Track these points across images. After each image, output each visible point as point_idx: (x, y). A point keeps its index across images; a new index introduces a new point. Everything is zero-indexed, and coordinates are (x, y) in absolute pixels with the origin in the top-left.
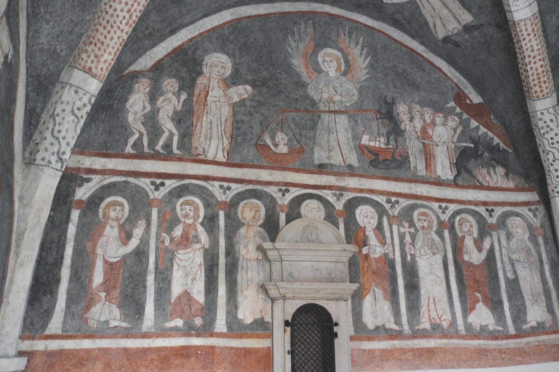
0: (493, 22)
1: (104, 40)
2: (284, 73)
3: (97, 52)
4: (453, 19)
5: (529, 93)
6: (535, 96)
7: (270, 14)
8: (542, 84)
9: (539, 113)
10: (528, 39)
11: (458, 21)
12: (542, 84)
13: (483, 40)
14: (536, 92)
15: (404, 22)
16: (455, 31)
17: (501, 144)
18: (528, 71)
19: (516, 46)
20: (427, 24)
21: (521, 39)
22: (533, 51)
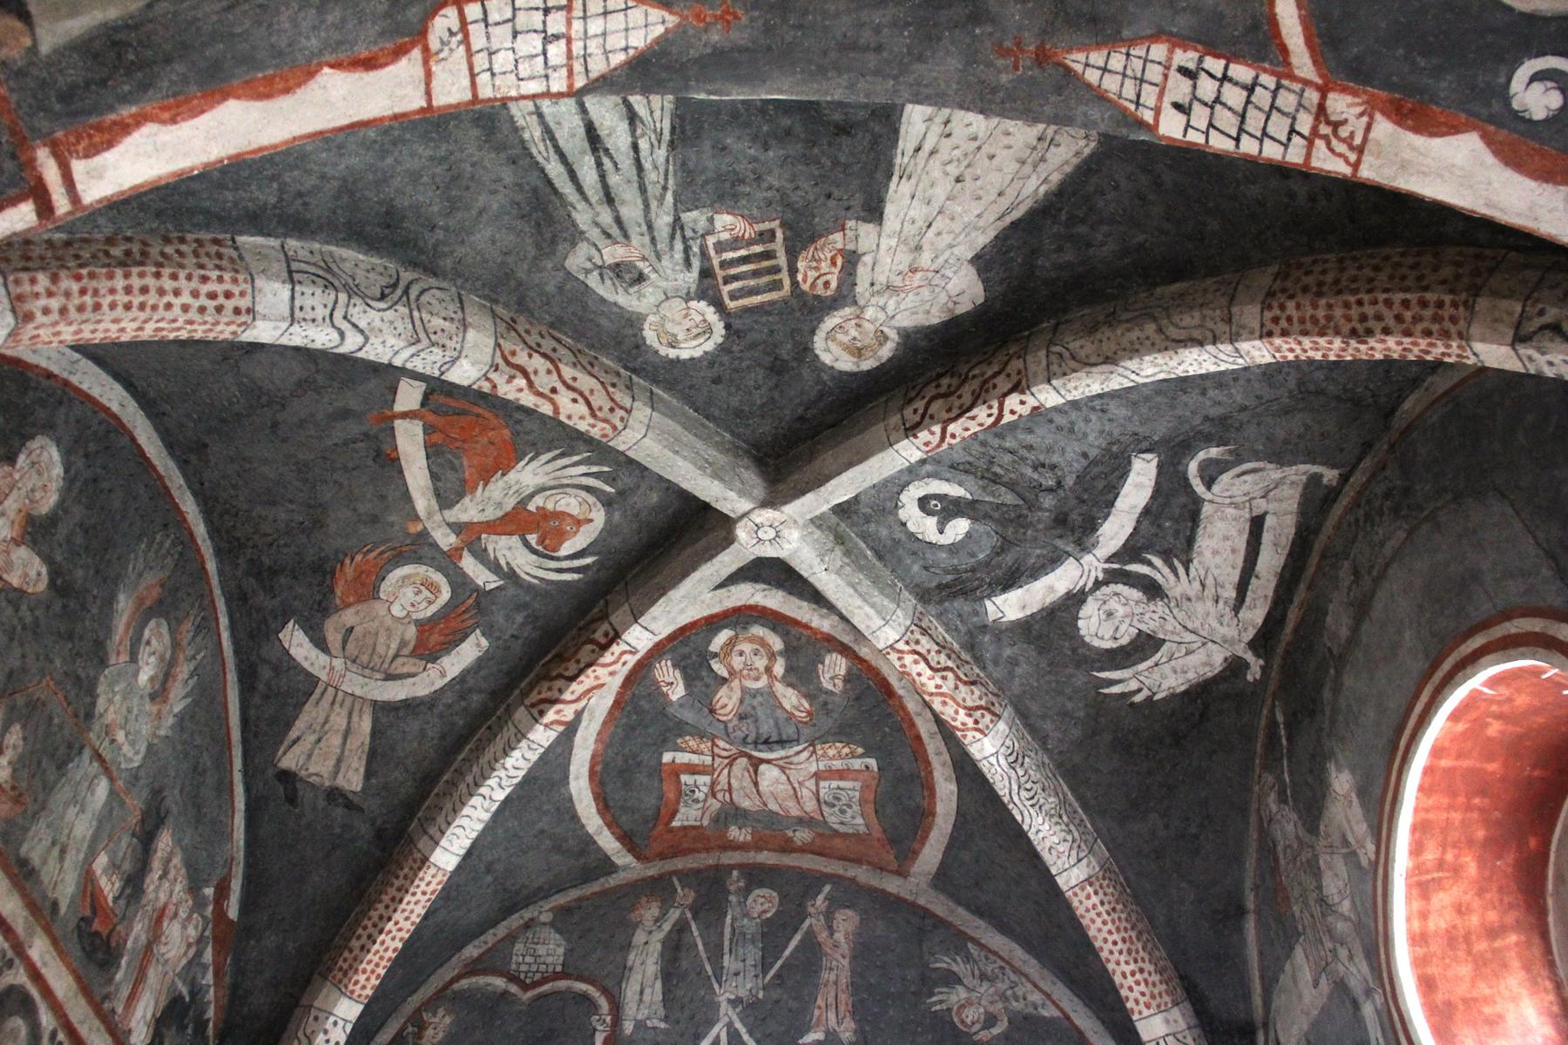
0: (379, 821)
1: (105, 307)
2: (98, 602)
3: (72, 309)
4: (332, 763)
5: (345, 974)
6: (351, 987)
7: (154, 468)
8: (373, 977)
9: (332, 1019)
10: (419, 896)
11: (336, 773)
12: (373, 977)
13: (338, 831)
14: (356, 983)
15: (261, 686)
16: (312, 779)
17: (211, 1025)
18: (374, 942)
19: (392, 892)
20: (289, 725)
21: (412, 890)
22: (407, 919)
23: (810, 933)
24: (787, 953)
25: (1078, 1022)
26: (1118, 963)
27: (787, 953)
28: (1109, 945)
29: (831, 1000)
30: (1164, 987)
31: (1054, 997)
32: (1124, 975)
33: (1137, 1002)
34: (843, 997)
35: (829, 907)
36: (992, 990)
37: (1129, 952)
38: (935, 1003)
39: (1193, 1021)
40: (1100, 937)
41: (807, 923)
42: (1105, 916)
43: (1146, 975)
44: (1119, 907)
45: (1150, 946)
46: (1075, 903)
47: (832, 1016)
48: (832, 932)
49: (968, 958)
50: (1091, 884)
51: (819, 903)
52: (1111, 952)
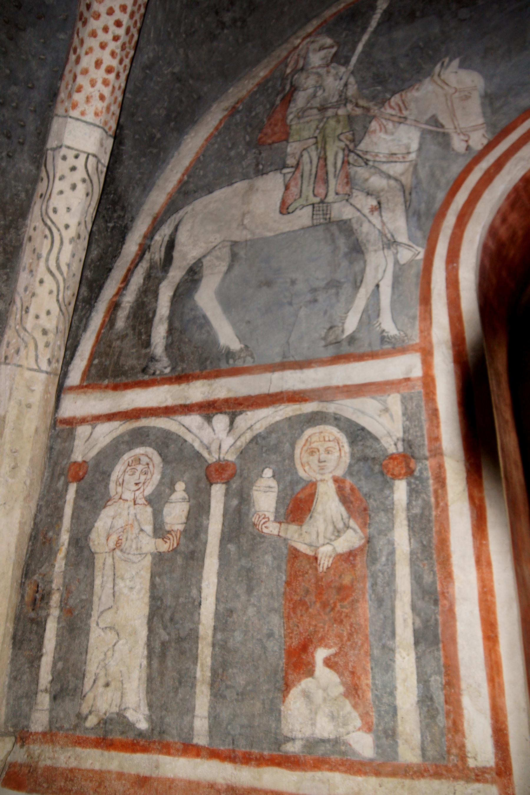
26: (103, 46)
28: (110, 21)
32: (98, 64)
33: (88, 100)
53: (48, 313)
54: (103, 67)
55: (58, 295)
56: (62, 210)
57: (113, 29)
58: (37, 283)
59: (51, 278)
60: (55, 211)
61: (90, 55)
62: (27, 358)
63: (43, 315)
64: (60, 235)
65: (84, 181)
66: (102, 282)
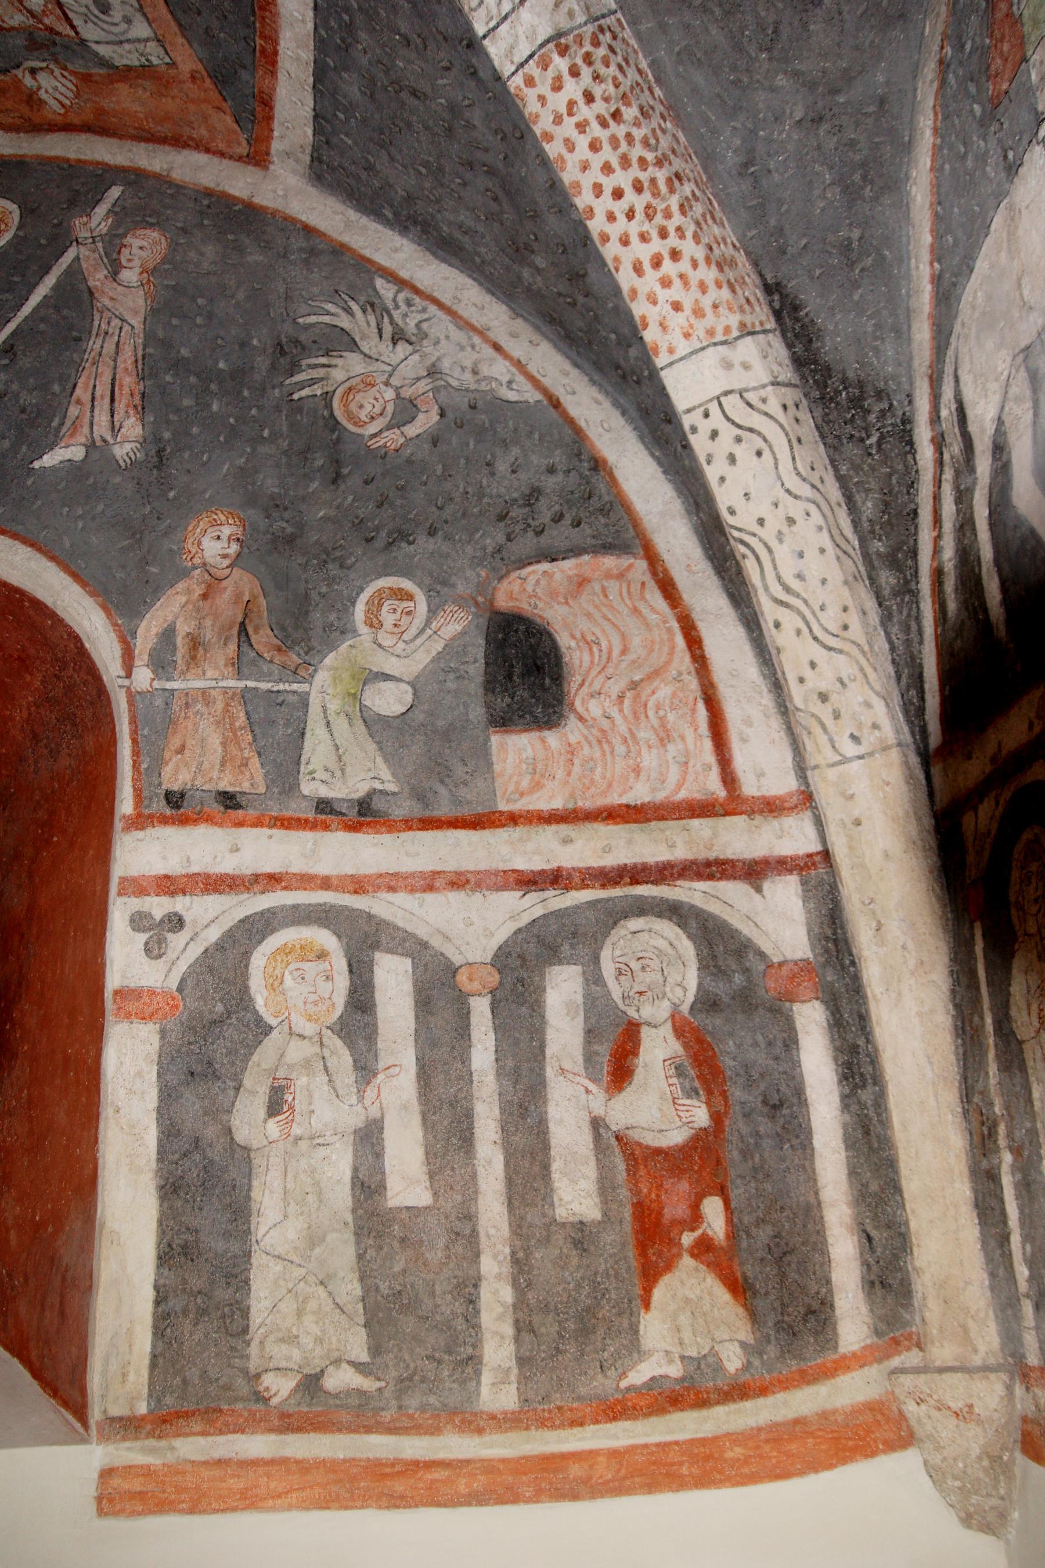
23: (74, 272)
24: (27, 309)
25: (574, 411)
26: (625, 242)
27: (27, 309)
29: (103, 389)
30: (725, 293)
31: (532, 369)
32: (638, 269)
34: (128, 382)
35: (111, 228)
36: (416, 357)
37: (650, 213)
38: (302, 385)
39: (787, 374)
40: (587, 182)
41: (71, 254)
42: (596, 130)
43: (684, 266)
44: (630, 113)
45: (698, 209)
46: (532, 107)
47: (102, 418)
48: (115, 270)
49: (372, 305)
50: (563, 51)
51: (93, 225)
52: (611, 217)
53: (813, 665)
54: (647, 266)
55: (811, 631)
56: (739, 504)
57: (619, 208)
58: (774, 631)
59: (787, 611)
60: (732, 512)
61: (621, 268)
62: (819, 751)
63: (808, 673)
64: (761, 540)
65: (738, 440)
66: (912, 542)
